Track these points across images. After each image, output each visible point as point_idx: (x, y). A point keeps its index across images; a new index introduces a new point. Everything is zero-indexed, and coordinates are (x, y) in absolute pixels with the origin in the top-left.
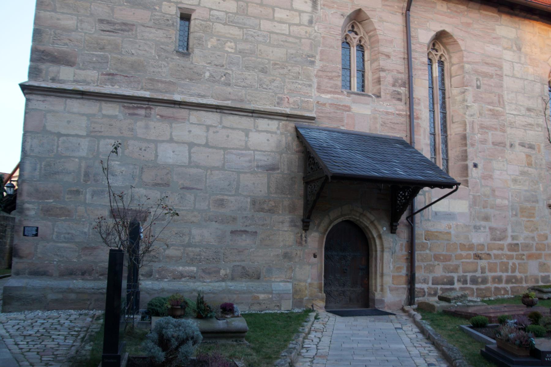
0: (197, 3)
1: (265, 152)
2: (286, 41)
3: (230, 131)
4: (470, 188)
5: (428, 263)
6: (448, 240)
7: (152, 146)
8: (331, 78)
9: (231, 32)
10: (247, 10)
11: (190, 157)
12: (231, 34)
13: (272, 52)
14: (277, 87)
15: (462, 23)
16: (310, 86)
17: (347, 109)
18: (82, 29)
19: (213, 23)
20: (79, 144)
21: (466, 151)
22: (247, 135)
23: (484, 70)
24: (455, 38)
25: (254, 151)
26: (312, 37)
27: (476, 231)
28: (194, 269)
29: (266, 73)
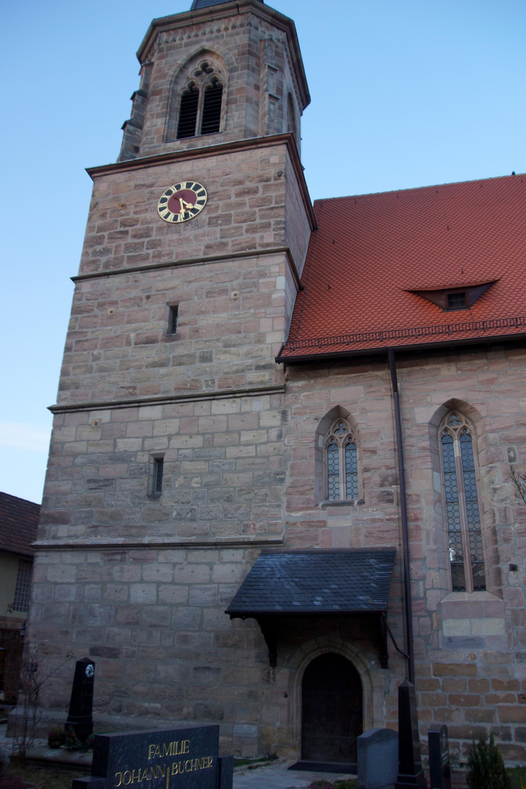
0: (167, 447)
1: (229, 583)
2: (253, 464)
3: (195, 566)
4: (506, 600)
5: (442, 707)
6: (471, 675)
7: (126, 587)
8: (302, 493)
9: (198, 467)
10: (213, 442)
11: (158, 596)
12: (198, 469)
13: (238, 478)
14: (243, 514)
15: (481, 382)
16: (279, 506)
17: (322, 524)
18: (75, 491)
19: (181, 462)
20: (70, 590)
21: (497, 549)
22: (211, 569)
23: (519, 435)
24: (471, 404)
25: (219, 583)
26: (281, 453)
27: (521, 662)
28: (158, 705)
29: (231, 501)
